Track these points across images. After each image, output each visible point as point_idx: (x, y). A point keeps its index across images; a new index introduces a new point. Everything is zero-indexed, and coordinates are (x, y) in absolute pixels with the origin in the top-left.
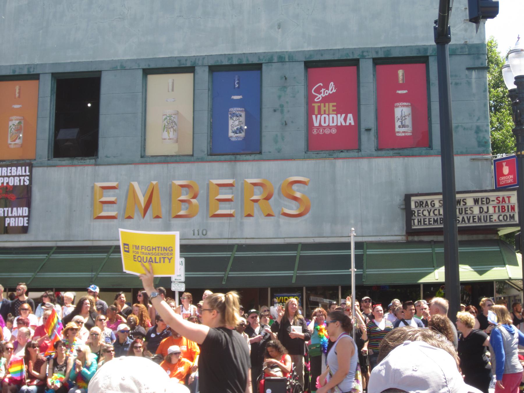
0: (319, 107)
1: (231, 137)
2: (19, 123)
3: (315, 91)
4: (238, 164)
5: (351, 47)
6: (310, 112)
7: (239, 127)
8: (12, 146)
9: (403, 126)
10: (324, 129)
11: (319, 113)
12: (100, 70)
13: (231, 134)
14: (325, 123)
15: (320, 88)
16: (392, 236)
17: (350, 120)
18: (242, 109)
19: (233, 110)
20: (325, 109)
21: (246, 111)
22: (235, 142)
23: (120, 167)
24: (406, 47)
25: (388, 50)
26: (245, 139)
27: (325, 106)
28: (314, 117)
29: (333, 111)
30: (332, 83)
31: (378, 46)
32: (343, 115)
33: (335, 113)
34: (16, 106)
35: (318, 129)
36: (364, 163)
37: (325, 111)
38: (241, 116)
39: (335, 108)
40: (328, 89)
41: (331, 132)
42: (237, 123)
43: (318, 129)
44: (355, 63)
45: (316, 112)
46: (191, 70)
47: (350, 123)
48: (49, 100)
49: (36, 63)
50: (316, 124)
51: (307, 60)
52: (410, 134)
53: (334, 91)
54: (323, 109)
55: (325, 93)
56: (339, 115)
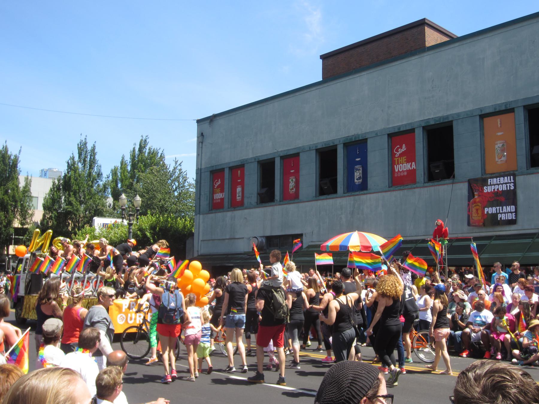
0: (398, 160)
1: (356, 182)
2: (503, 145)
3: (396, 151)
4: (217, 214)
5: (245, 158)
6: (392, 163)
7: (359, 176)
8: (291, 193)
9: (239, 196)
10: (401, 173)
11: (398, 164)
12: (273, 157)
13: (356, 181)
14: (401, 169)
15: (398, 148)
16: (424, 235)
17: (414, 166)
18: (361, 166)
19: (357, 167)
20: (401, 161)
21: (363, 167)
22: (359, 185)
23: (342, 199)
24: (264, 155)
25: (399, 127)
26: (362, 182)
27: (401, 159)
28: (395, 166)
29: (405, 161)
30: (404, 145)
31: (454, 112)
32: (410, 163)
33: (406, 162)
34: (292, 171)
35: (397, 173)
36: (339, 201)
37: (401, 162)
38: (360, 170)
39: (406, 160)
40: (402, 149)
41: (404, 175)
42: (358, 174)
43: (397, 173)
44: (412, 131)
45: (396, 163)
46: (512, 110)
47: (414, 168)
48: (387, 151)
49: (356, 134)
50: (397, 170)
51: (345, 142)
52: (240, 200)
53: (405, 149)
54: (400, 161)
55: (401, 151)
56: (408, 164)
